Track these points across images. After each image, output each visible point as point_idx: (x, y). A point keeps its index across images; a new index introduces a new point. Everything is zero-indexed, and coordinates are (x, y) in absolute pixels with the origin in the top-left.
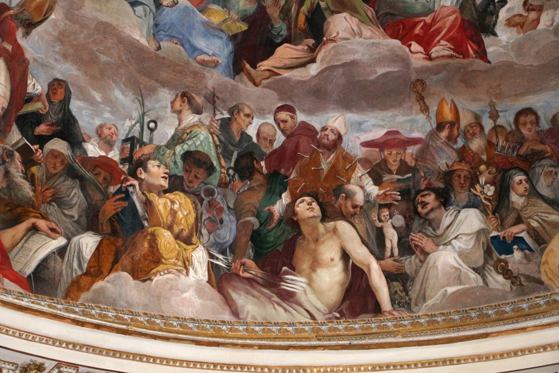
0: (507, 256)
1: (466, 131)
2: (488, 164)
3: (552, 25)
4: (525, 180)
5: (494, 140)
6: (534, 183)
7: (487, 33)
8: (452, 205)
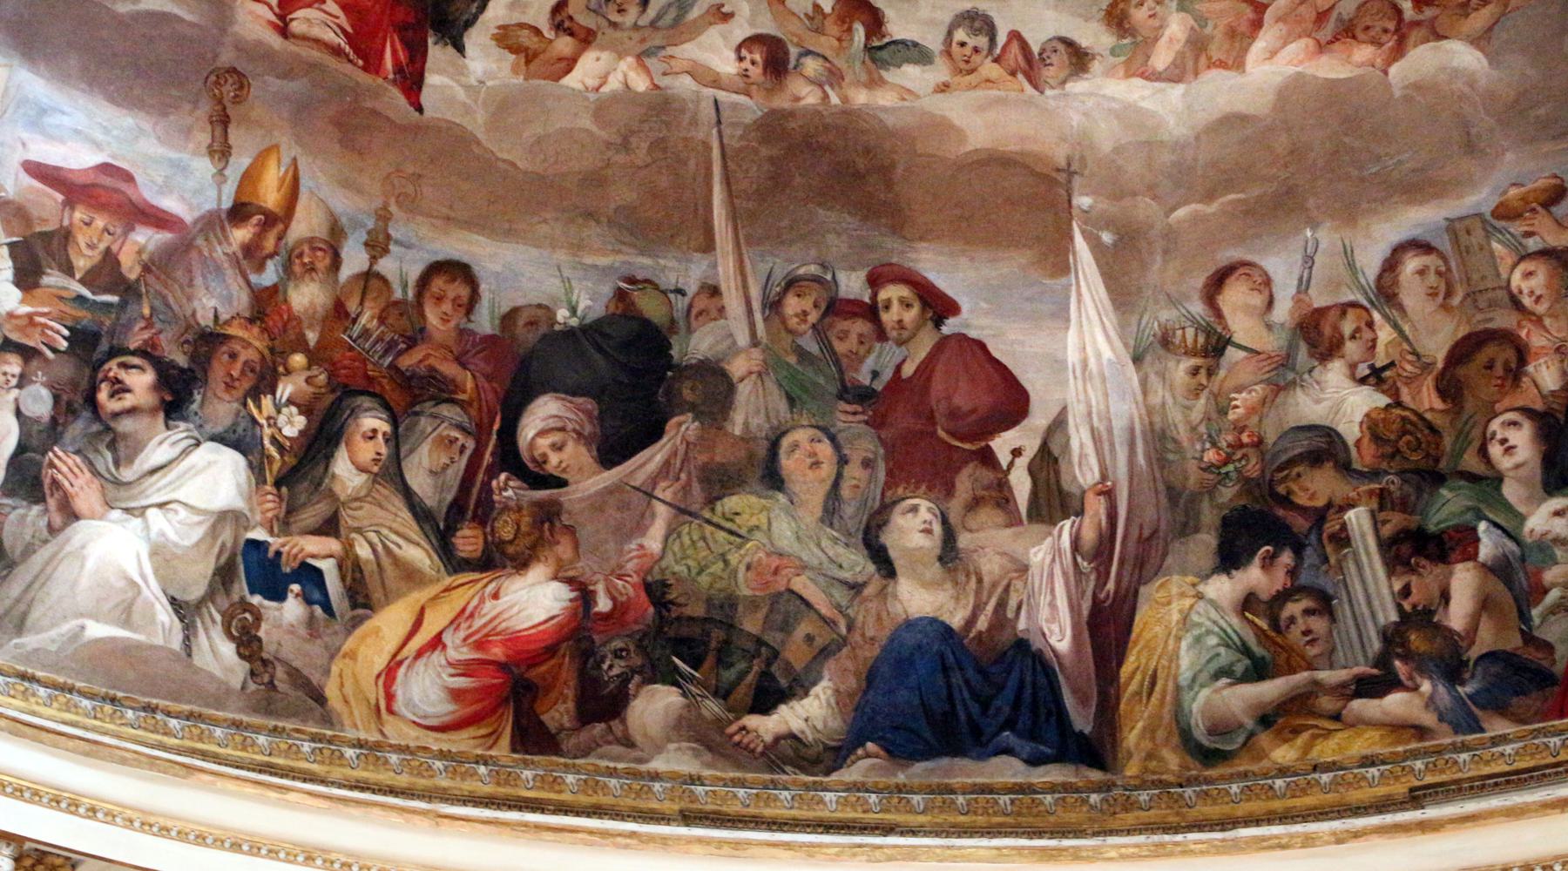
0: (266, 603)
1: (297, 252)
2: (314, 358)
3: (597, 90)
4: (384, 434)
5: (352, 306)
6: (404, 450)
7: (443, 37)
8: (185, 419)
